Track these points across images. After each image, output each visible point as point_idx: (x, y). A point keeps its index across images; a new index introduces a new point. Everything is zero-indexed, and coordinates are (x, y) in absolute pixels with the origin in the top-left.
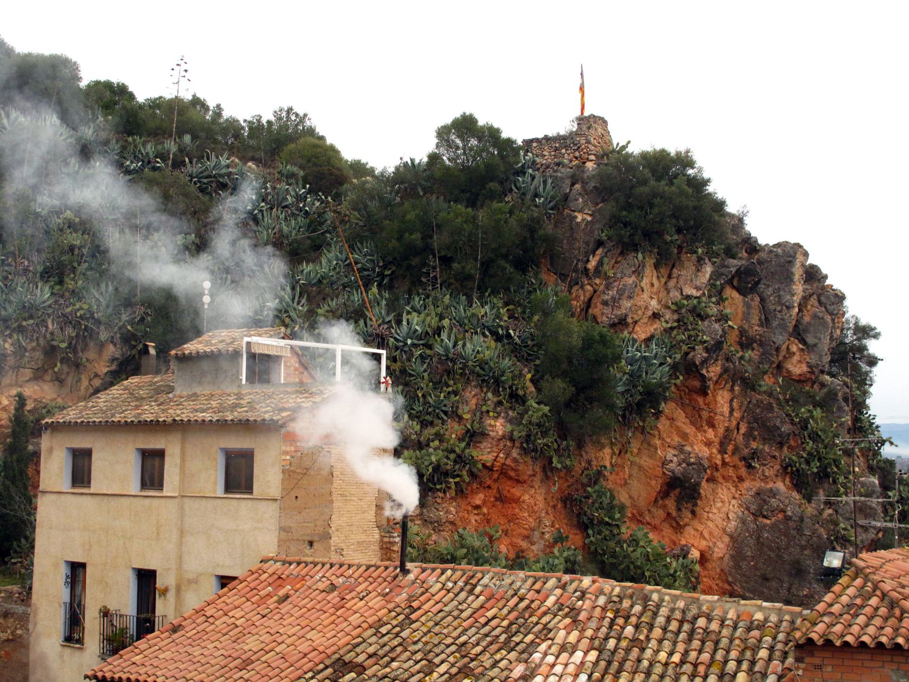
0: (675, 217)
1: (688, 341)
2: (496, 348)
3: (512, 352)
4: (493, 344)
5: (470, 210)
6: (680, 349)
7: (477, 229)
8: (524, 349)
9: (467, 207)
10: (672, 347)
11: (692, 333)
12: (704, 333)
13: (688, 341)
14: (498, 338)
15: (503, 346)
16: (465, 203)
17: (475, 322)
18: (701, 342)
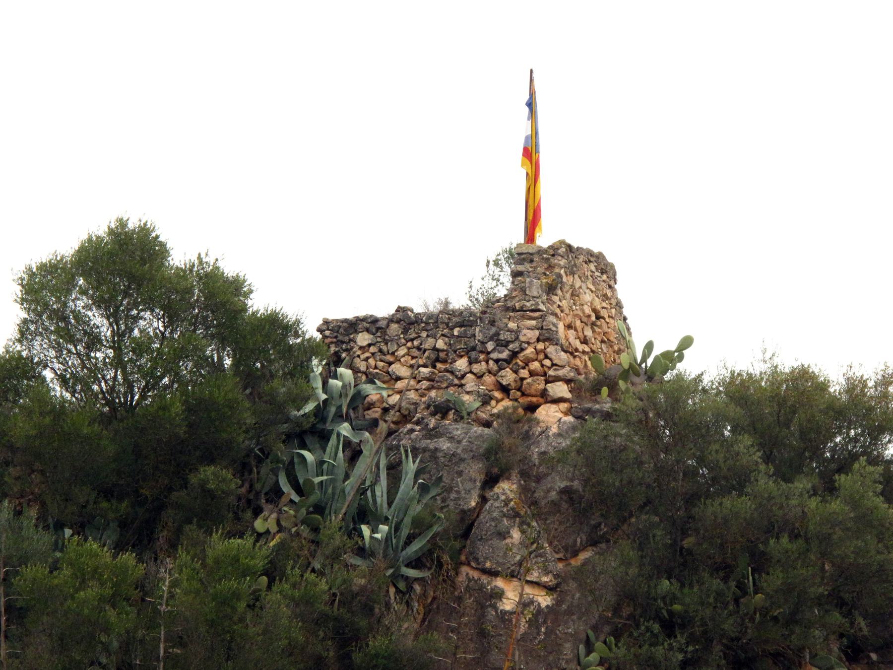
0: (841, 604)
5: (128, 558)
7: (152, 626)
9: (119, 547)
16: (111, 536)
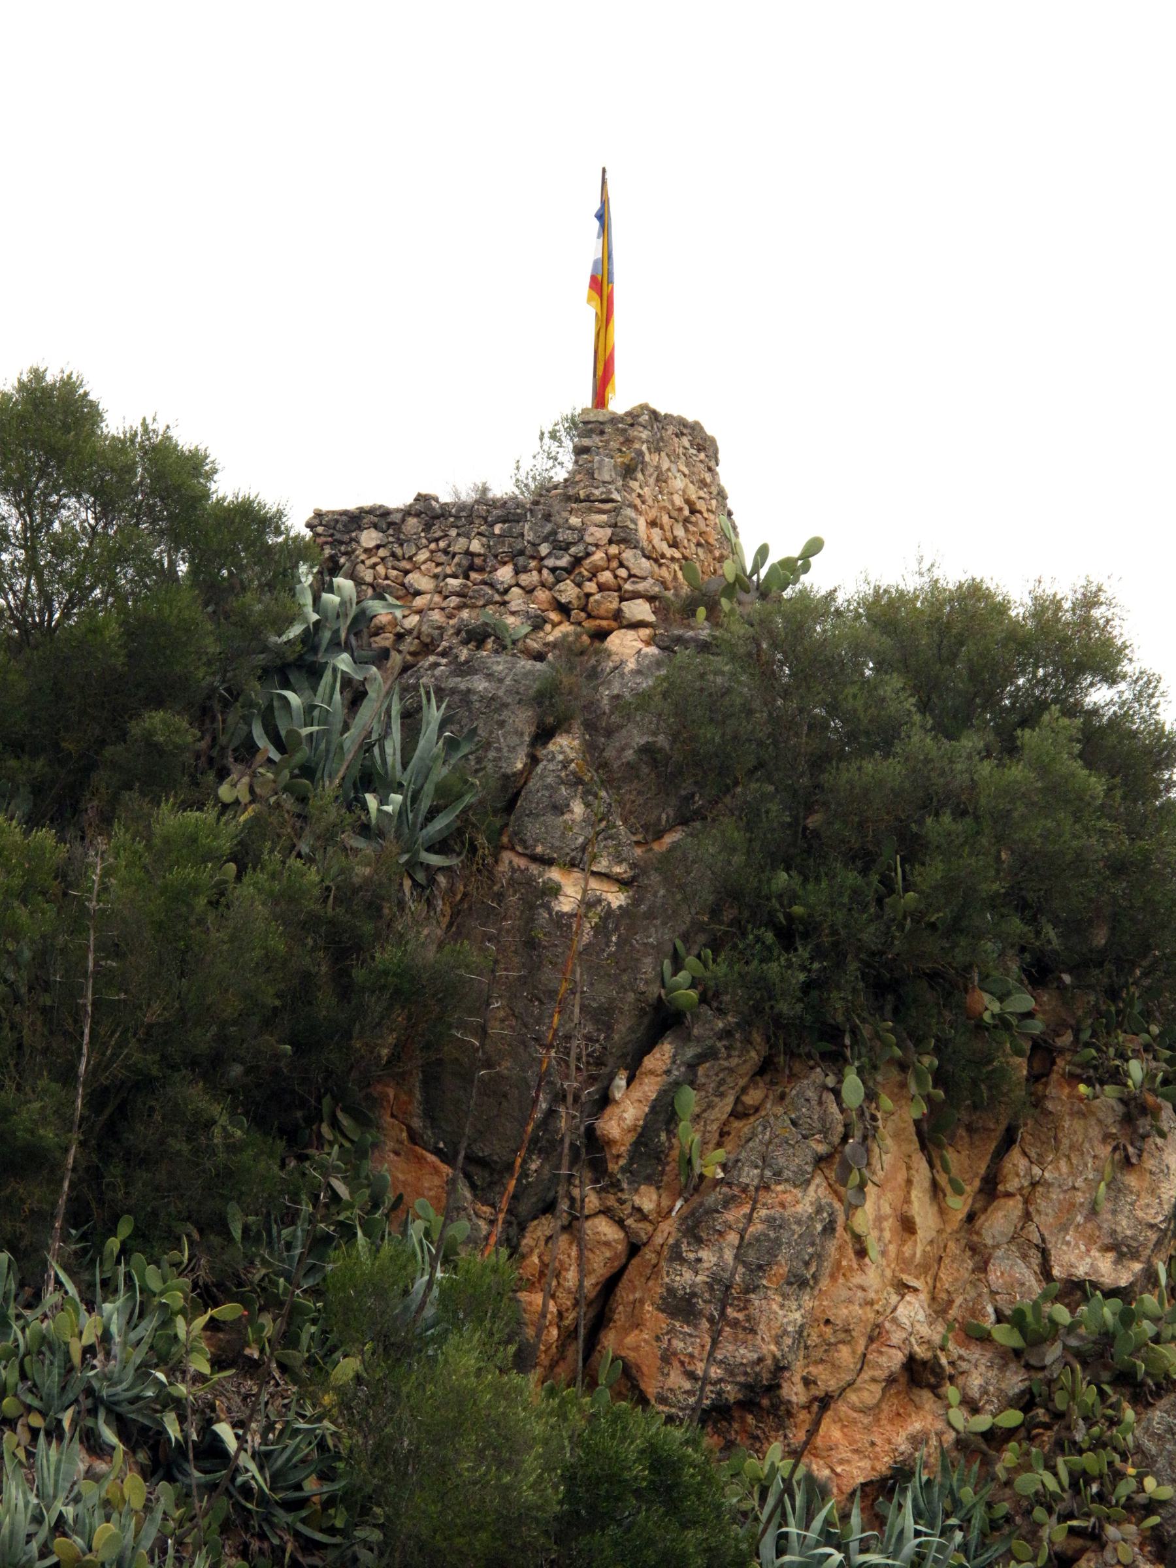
0: (1023, 907)
1: (1068, 1501)
2: (148, 1508)
3: (226, 1528)
4: (134, 1488)
5: (45, 836)
6: (1033, 1535)
7: (77, 928)
8: (283, 1517)
9: (32, 822)
10: (994, 1526)
11: (1089, 1461)
12: (1147, 1465)
13: (1068, 1501)
14: (160, 1463)
15: (183, 1499)
16: (21, 806)
17: (51, 1380)
18: (1130, 1505)
